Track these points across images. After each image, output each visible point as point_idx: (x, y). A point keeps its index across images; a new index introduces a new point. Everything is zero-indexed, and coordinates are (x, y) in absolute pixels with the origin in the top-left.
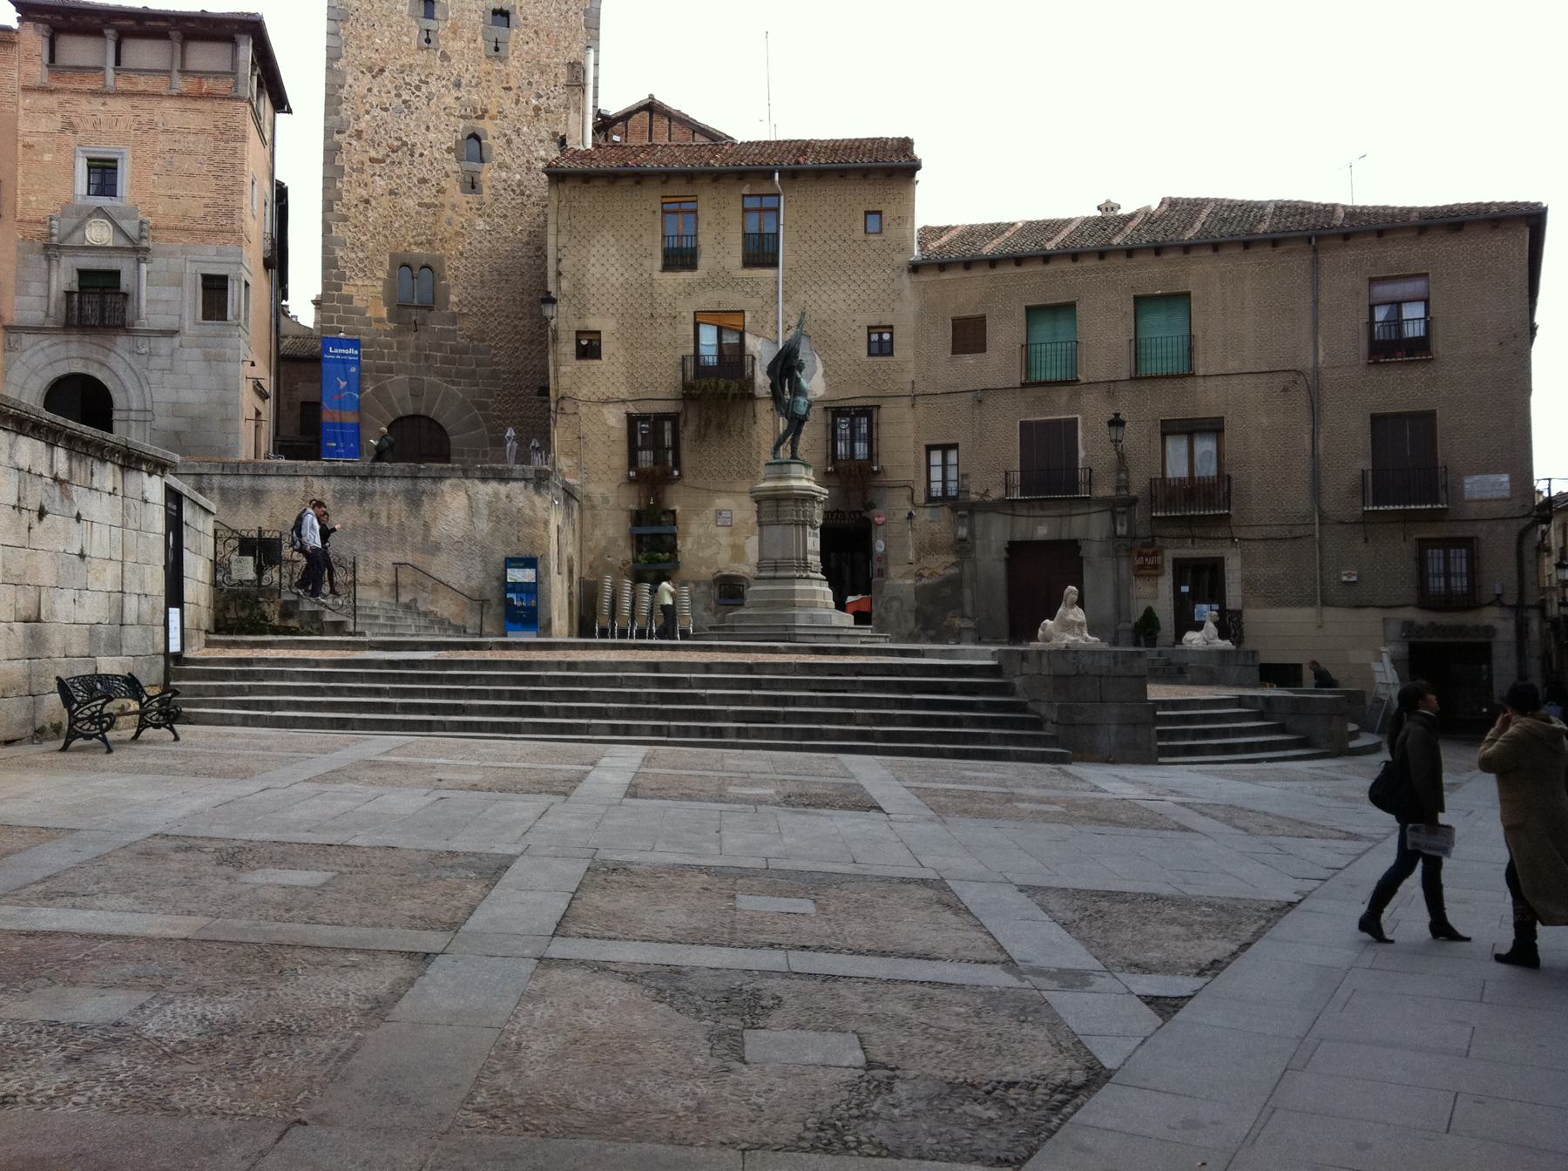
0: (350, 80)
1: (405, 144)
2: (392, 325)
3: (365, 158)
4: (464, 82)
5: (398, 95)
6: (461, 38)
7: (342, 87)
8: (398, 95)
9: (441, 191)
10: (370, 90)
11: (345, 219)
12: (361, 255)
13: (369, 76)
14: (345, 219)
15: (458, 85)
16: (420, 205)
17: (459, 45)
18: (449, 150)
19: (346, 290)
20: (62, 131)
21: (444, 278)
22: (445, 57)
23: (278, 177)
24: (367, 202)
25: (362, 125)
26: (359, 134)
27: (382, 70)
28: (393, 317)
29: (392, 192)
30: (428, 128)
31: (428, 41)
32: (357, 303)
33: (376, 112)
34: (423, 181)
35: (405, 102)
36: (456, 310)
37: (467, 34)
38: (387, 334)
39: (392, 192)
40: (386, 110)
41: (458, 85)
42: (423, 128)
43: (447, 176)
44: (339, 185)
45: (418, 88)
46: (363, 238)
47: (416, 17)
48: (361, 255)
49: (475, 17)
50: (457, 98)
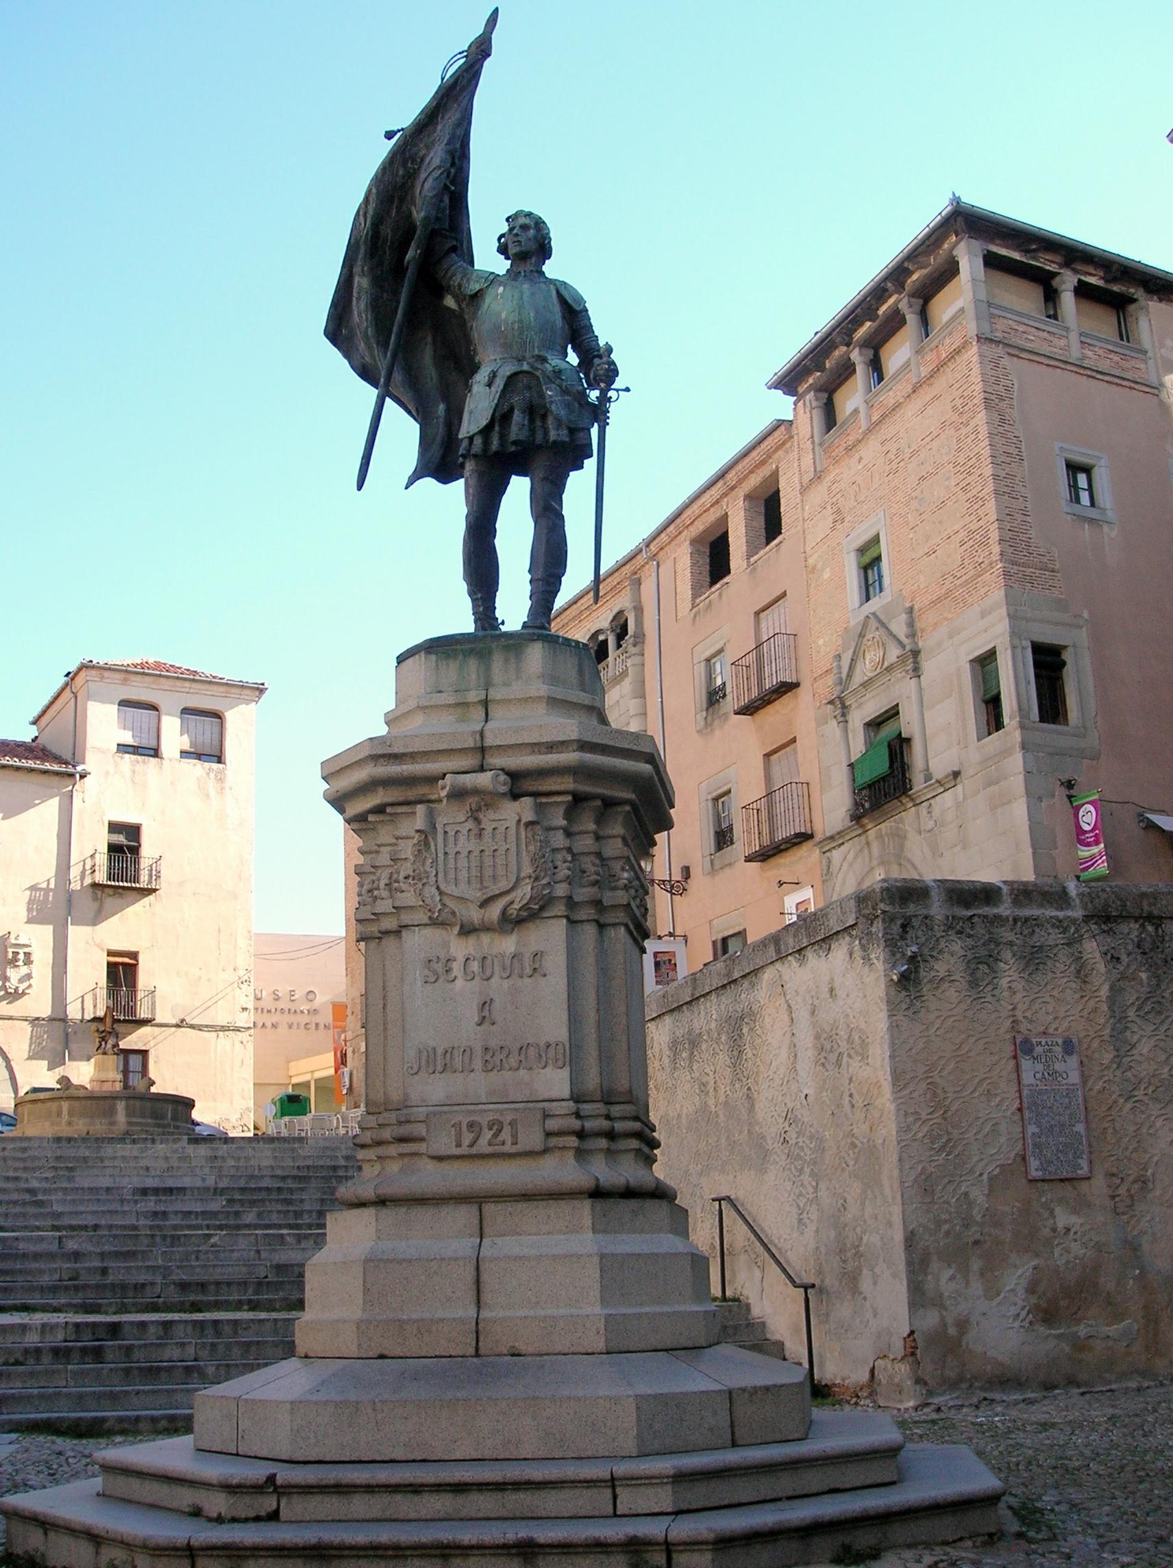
20: (833, 529)
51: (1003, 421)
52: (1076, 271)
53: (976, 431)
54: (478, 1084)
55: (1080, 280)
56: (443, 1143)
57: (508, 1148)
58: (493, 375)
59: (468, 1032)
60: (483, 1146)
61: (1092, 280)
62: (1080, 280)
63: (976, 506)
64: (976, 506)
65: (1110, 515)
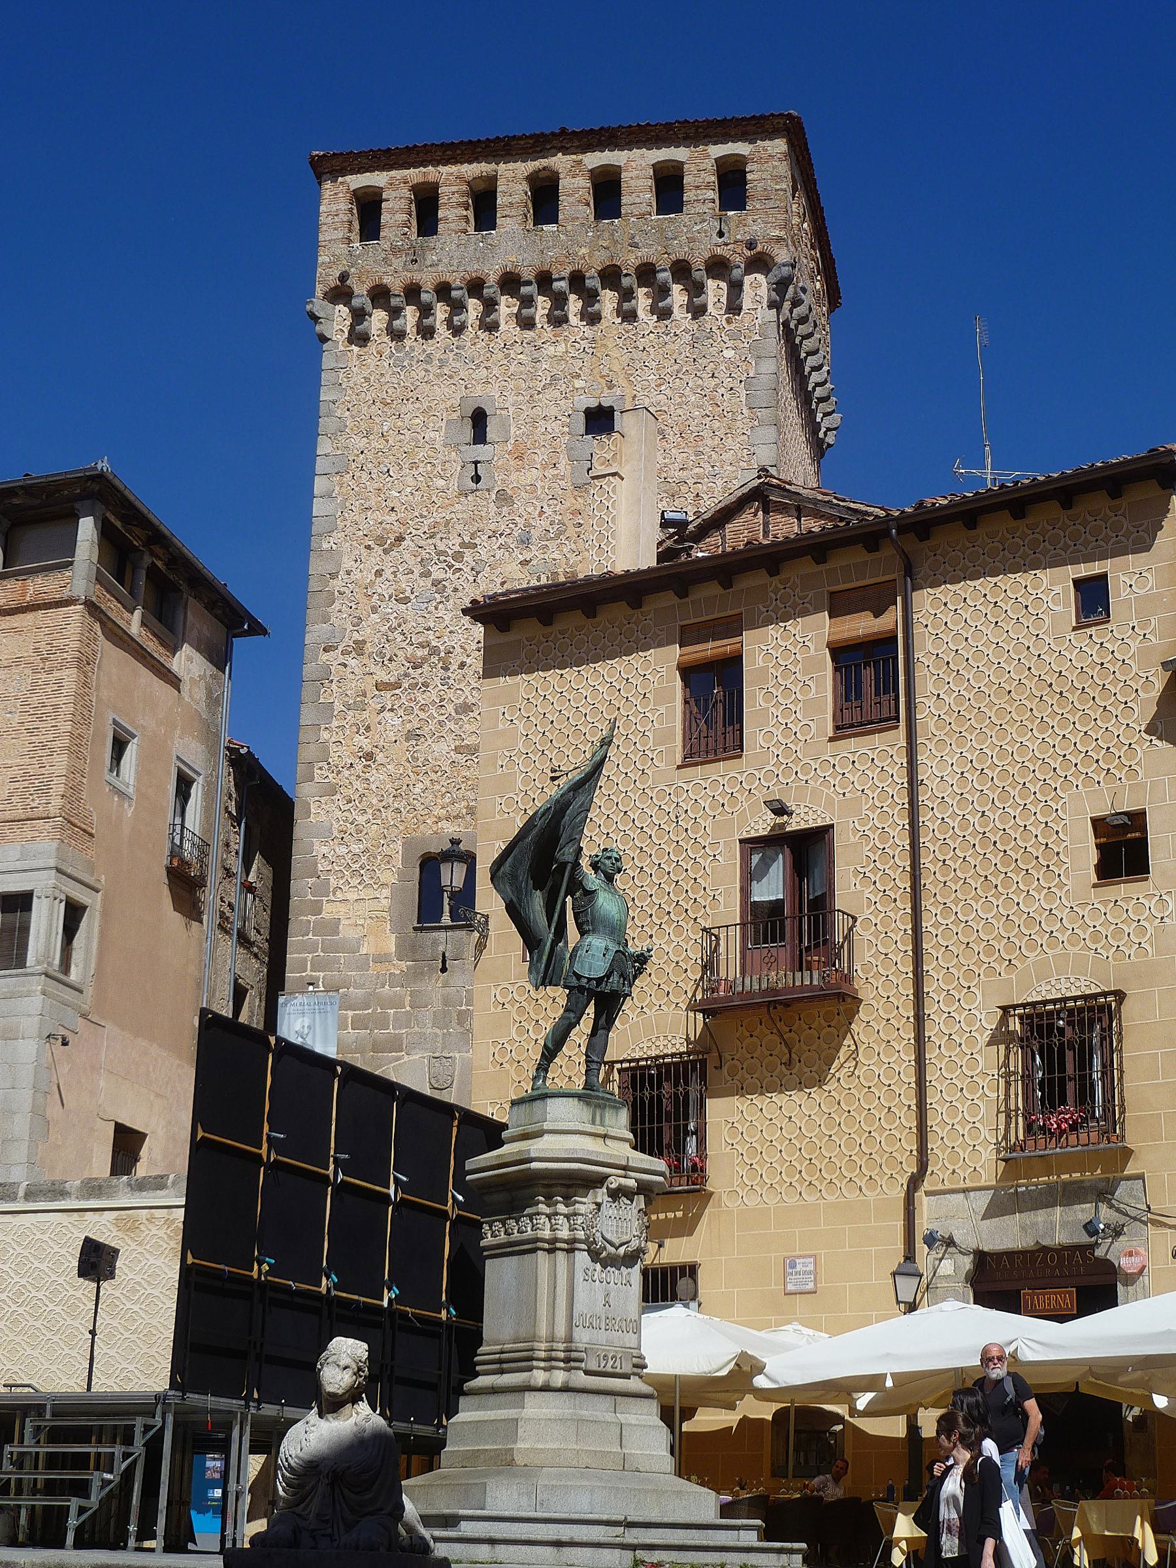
0: (347, 563)
1: (434, 651)
2: (404, 965)
4: (535, 534)
5: (426, 574)
7: (334, 576)
8: (426, 574)
10: (379, 573)
11: (332, 790)
12: (356, 848)
13: (380, 550)
14: (332, 790)
15: (525, 542)
16: (457, 750)
19: (329, 911)
22: (503, 498)
24: (369, 756)
25: (366, 632)
26: (359, 647)
27: (400, 539)
28: (407, 950)
31: (477, 479)
32: (347, 932)
35: (436, 583)
37: (541, 456)
38: (393, 980)
39: (413, 736)
40: (406, 601)
41: (525, 542)
45: (458, 556)
46: (361, 819)
49: (556, 427)
50: (525, 563)
51: (85, 684)
52: (152, 554)
53: (59, 683)
54: (602, 1336)
56: (593, 1366)
57: (618, 1370)
58: (607, 949)
59: (599, 1309)
60: (609, 1369)
61: (159, 564)
63: (40, 753)
64: (40, 753)
65: (131, 790)
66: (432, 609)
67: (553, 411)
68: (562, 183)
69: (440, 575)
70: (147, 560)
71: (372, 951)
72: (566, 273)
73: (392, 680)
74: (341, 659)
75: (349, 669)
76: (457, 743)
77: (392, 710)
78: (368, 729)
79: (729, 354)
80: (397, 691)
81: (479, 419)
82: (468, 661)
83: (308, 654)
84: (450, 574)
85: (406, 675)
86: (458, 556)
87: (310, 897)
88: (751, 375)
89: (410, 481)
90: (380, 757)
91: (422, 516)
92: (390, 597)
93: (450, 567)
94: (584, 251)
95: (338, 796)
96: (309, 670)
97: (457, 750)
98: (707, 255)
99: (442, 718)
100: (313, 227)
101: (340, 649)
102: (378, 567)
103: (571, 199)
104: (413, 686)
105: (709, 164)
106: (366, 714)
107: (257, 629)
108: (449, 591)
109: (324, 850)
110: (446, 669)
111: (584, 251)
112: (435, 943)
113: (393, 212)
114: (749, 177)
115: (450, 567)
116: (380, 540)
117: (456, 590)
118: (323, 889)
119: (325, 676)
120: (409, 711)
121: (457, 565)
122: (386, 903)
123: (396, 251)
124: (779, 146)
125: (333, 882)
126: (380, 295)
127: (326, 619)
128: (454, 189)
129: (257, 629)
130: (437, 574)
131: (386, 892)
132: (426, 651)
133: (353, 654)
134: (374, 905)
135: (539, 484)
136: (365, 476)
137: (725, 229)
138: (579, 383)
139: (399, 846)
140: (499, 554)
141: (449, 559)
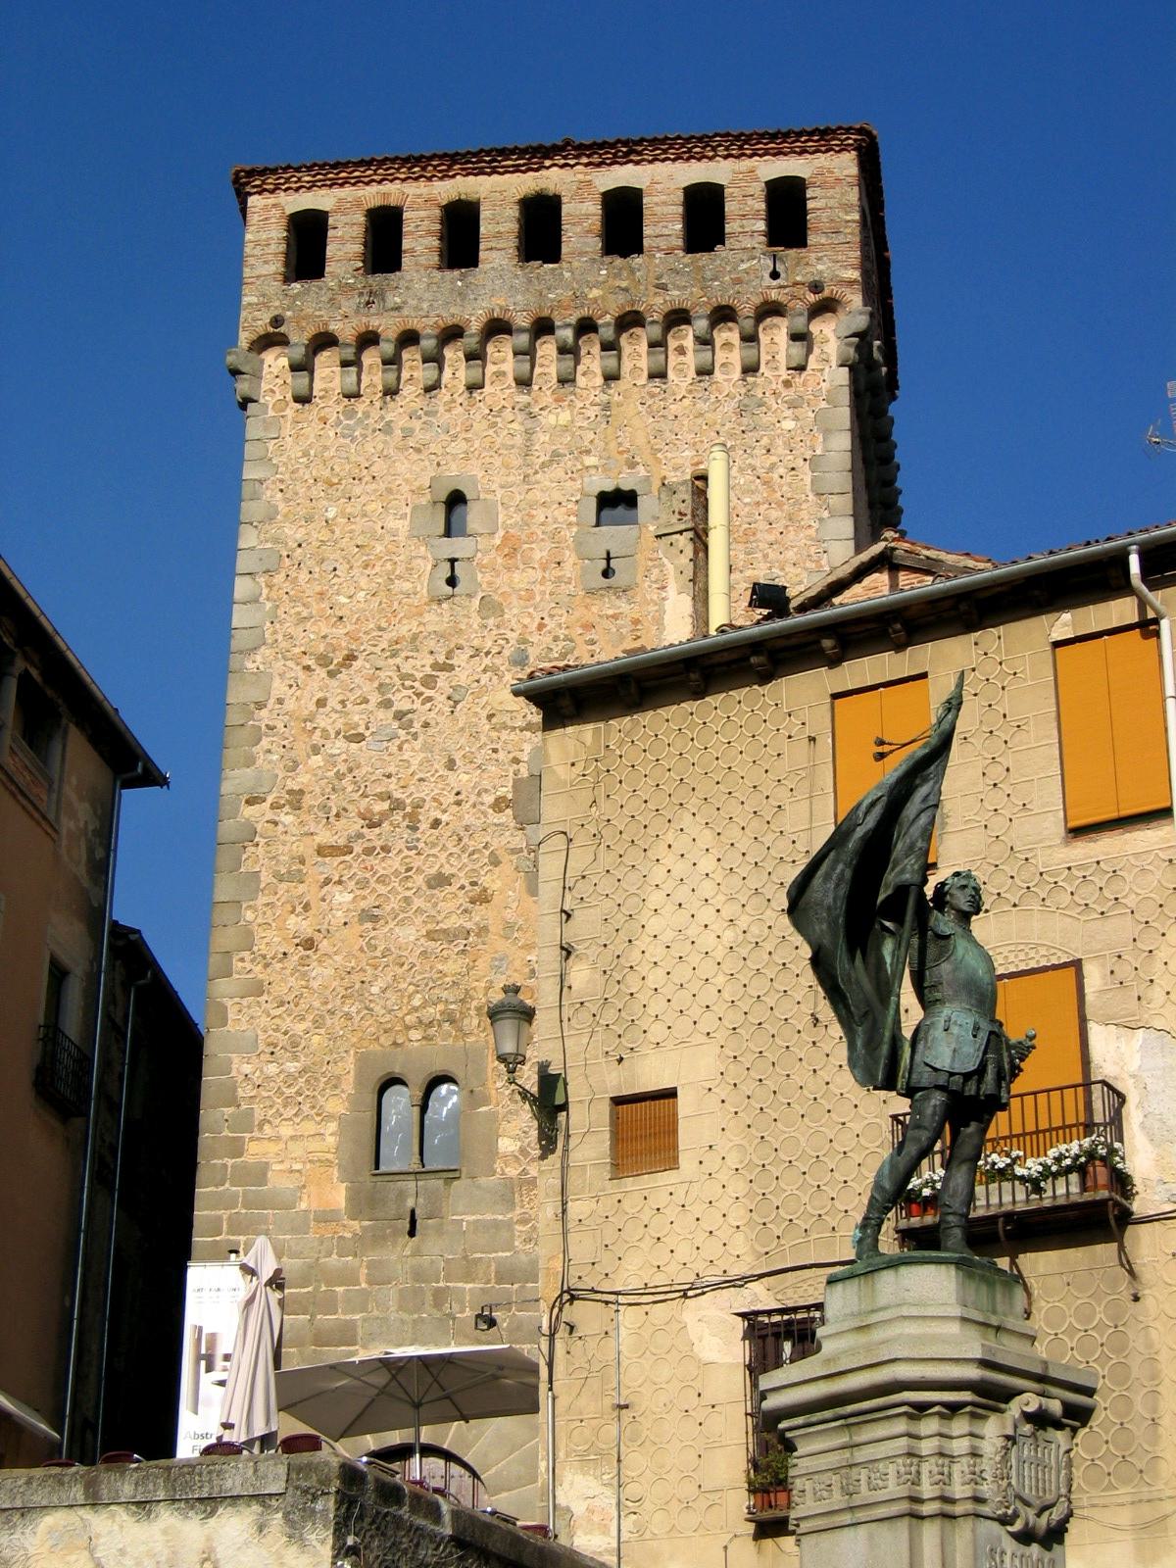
0: (279, 688)
1: (398, 805)
2: (356, 1225)
3: (306, 848)
5: (387, 704)
6: (527, 563)
7: (260, 705)
8: (387, 704)
9: (483, 898)
11: (258, 989)
12: (292, 1067)
13: (321, 672)
14: (258, 989)
16: (430, 936)
17: (521, 579)
18: (499, 805)
19: (255, 1151)
21: (486, 1101)
22: (490, 607)
23: (123, 912)
24: (309, 944)
26: (296, 799)
27: (351, 657)
28: (362, 1203)
29: (370, 917)
30: (451, 765)
31: (452, 581)
32: (278, 1181)
33: (339, 746)
34: (440, 880)
35: (399, 716)
36: (512, 1172)
39: (370, 917)
40: (359, 738)
42: (439, 766)
43: (495, 862)
44: (249, 915)
45: (429, 681)
47: (425, 540)
48: (292, 1067)
49: (560, 514)
52: (27, 658)
55: (26, 670)
61: (34, 673)
62: (26, 670)
66: (394, 749)
67: (557, 496)
68: (565, 209)
69: (405, 706)
70: (20, 665)
71: (314, 1207)
72: (573, 320)
73: (342, 842)
74: (270, 815)
75: (280, 828)
76: (430, 927)
77: (340, 882)
78: (307, 907)
79: (788, 424)
80: (348, 858)
81: (456, 500)
82: (444, 818)
83: (225, 808)
84: (417, 705)
85: (360, 836)
86: (429, 681)
87: (226, 1133)
88: (818, 452)
89: (363, 582)
90: (324, 946)
91: (380, 629)
92: (338, 733)
93: (419, 695)
94: (595, 293)
95: (265, 997)
96: (227, 828)
97: (430, 936)
98: (757, 300)
99: (409, 893)
100: (235, 258)
101: (270, 799)
102: (320, 695)
103: (578, 229)
104: (368, 851)
105: (758, 189)
106: (302, 888)
107: (152, 777)
108: (417, 726)
109: (247, 1069)
110: (414, 829)
111: (595, 293)
112: (402, 1196)
113: (342, 241)
114: (810, 205)
115: (419, 695)
116: (324, 660)
117: (426, 725)
118: (245, 1122)
119: (730, 329)
120: (363, 884)
121: (428, 693)
122: (331, 1140)
123: (345, 288)
124: (846, 164)
125: (258, 1115)
126: (324, 341)
127: (250, 761)
128: (423, 214)
129: (152, 777)
130: (401, 704)
131: (333, 1126)
132: (386, 805)
133: (287, 809)
134: (314, 1145)
135: (537, 588)
136: (303, 576)
137: (780, 268)
138: (590, 461)
139: (350, 1063)
140: (484, 679)
141: (417, 684)
